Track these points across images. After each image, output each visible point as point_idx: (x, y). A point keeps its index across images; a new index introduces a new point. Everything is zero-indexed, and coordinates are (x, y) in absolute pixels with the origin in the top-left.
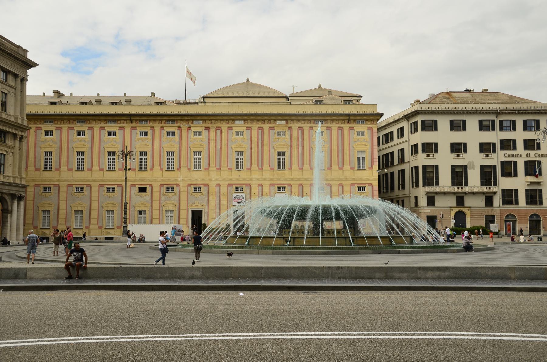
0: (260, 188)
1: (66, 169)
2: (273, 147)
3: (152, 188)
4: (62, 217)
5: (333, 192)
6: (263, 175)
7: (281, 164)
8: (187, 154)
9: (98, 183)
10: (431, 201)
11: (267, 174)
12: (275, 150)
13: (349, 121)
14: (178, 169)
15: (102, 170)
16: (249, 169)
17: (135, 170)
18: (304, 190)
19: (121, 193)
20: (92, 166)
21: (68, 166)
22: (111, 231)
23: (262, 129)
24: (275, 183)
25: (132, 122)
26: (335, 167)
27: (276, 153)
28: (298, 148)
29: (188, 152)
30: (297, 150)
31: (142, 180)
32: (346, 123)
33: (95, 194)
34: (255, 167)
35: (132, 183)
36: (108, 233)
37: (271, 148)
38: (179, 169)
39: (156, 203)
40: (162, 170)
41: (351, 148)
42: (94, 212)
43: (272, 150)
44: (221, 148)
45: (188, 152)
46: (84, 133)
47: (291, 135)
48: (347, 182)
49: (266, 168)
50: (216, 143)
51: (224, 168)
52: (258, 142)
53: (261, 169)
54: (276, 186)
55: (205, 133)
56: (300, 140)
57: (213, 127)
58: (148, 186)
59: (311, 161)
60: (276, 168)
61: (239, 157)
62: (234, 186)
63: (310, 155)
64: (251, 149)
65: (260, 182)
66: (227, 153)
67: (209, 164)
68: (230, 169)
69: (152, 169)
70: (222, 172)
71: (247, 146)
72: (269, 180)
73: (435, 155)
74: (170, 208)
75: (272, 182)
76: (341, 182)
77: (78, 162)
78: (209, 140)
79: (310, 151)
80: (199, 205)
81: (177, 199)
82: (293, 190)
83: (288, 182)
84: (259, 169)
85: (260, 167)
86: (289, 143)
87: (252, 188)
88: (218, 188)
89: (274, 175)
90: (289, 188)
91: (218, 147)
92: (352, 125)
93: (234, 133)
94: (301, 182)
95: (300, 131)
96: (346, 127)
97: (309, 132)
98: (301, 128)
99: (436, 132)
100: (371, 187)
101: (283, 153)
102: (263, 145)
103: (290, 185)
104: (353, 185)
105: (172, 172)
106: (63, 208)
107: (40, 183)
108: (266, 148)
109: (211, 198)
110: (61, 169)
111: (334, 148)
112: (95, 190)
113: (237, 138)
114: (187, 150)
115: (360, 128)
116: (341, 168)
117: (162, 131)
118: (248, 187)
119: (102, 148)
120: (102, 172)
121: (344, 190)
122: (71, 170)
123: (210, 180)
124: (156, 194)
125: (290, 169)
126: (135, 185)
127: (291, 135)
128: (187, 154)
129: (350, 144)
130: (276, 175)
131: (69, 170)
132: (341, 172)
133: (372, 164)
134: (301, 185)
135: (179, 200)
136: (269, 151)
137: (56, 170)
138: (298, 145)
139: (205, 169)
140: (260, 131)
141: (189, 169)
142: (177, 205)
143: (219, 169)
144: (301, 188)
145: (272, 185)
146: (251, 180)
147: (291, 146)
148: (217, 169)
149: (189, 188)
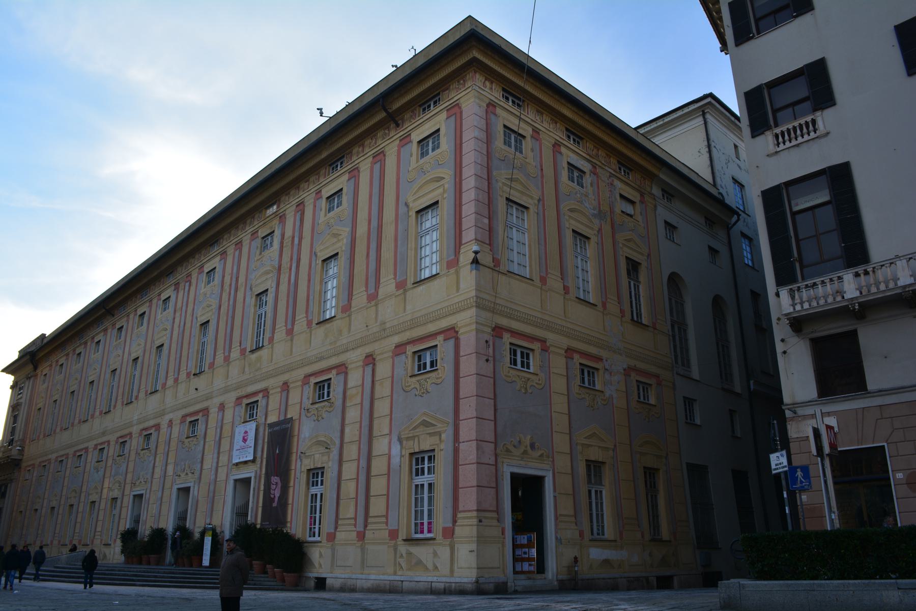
2: (251, 289)
5: (349, 393)
6: (227, 377)
10: (840, 370)
13: (394, 119)
25: (113, 316)
26: (360, 298)
28: (290, 269)
30: (287, 275)
41: (402, 209)
47: (283, 235)
52: (230, 285)
59: (311, 297)
63: (309, 281)
70: (179, 386)
73: (825, 119)
76: (368, 349)
78: (175, 311)
91: (182, 323)
99: (807, 19)
100: (451, 342)
104: (400, 349)
109: (157, 459)
111: (362, 230)
116: (373, 297)
123: (162, 414)
127: (283, 235)
133: (458, 244)
138: (291, 259)
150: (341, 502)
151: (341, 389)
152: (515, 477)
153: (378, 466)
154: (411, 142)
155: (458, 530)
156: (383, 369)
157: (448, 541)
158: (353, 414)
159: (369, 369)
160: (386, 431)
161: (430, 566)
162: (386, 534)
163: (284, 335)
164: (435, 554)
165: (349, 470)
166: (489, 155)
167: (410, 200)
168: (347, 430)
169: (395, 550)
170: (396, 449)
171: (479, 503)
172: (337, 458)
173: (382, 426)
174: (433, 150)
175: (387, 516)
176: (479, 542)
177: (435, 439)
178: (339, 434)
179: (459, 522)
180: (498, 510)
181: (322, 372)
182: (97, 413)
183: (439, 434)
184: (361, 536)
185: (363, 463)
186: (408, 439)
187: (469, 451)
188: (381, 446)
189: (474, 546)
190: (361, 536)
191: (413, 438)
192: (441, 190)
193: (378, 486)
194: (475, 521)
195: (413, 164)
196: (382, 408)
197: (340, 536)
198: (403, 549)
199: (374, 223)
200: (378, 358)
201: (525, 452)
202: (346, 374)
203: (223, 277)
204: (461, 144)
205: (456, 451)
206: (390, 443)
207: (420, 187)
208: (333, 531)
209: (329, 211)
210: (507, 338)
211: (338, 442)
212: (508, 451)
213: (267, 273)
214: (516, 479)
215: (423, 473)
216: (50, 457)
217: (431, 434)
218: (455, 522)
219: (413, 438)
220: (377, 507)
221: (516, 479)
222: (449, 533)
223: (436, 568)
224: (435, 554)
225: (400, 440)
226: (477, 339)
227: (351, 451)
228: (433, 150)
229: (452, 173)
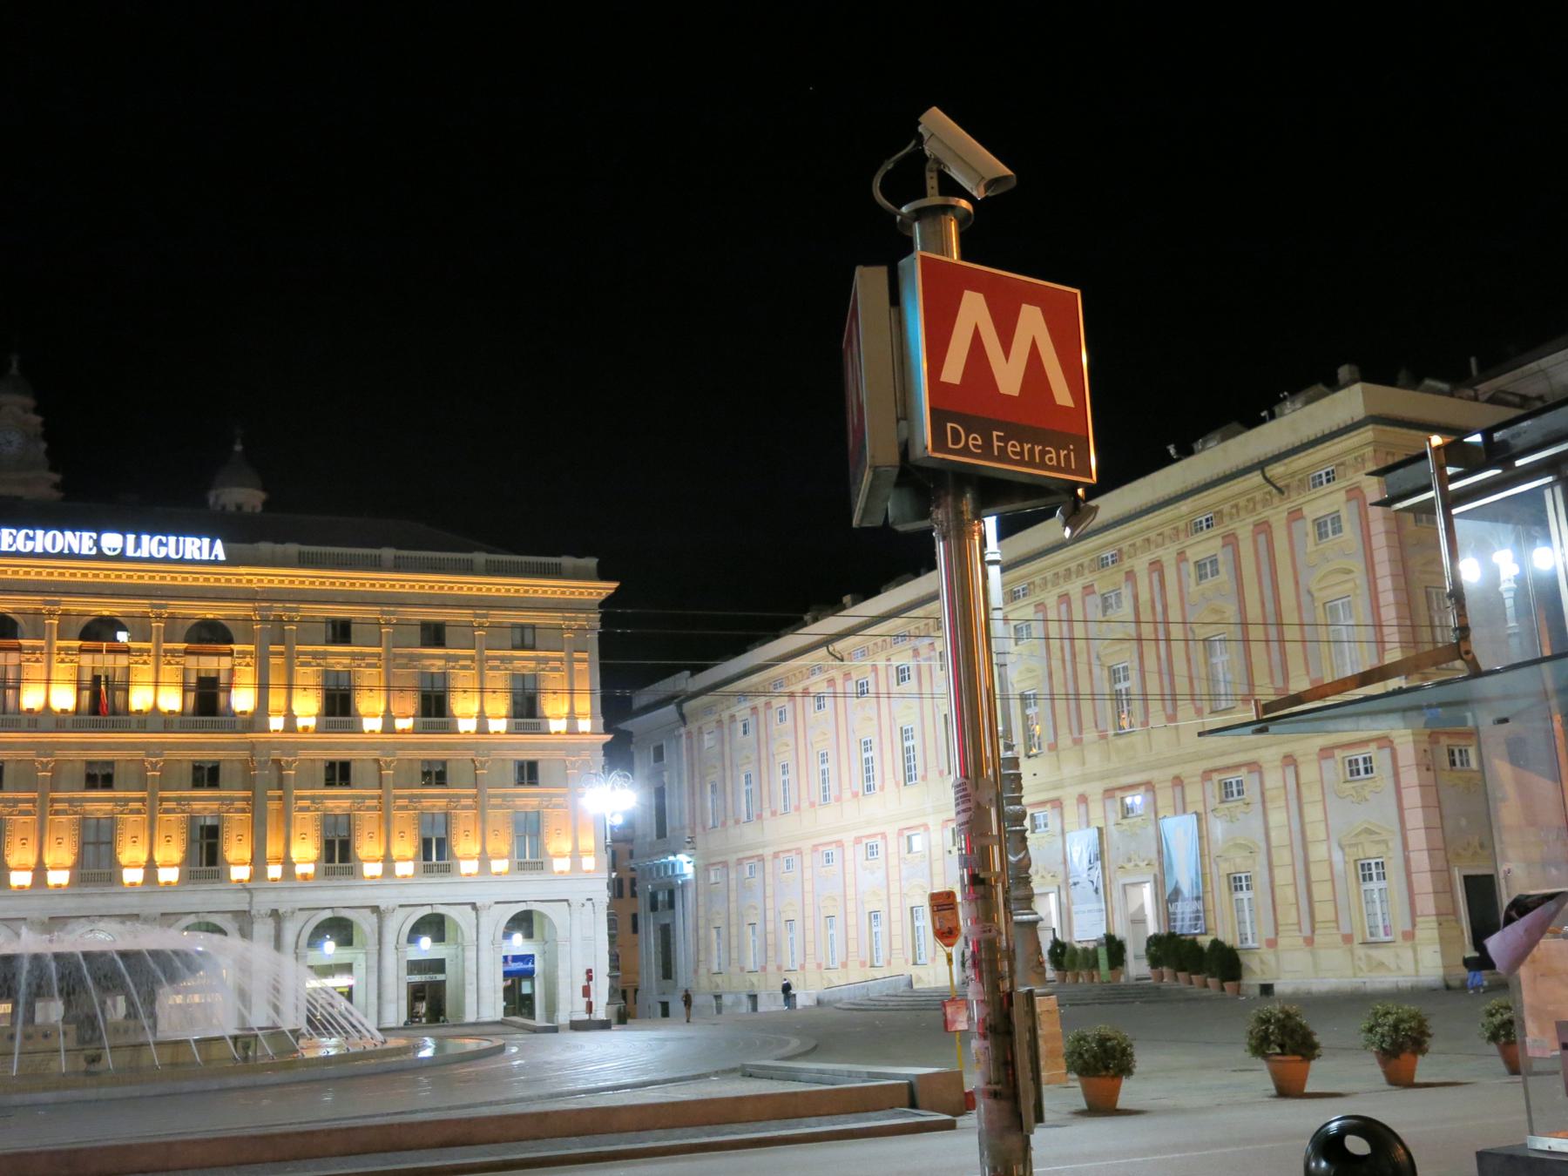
2: (1098, 658)
4: (770, 938)
5: (1268, 794)
18: (1188, 799)
27: (1106, 672)
32: (1276, 500)
34: (1065, 740)
35: (855, 834)
37: (1093, 656)
39: (894, 888)
40: (897, 784)
41: (1305, 599)
42: (809, 924)
43: (1096, 670)
47: (1136, 598)
49: (1090, 735)
58: (879, 841)
60: (1111, 732)
63: (1189, 660)
69: (882, 788)
72: (1102, 778)
82: (1159, 804)
85: (1076, 735)
94: (1175, 771)
96: (1277, 514)
97: (1179, 570)
98: (1157, 566)
100: (1387, 752)
106: (770, 915)
107: (741, 855)
115: (1322, 502)
118: (1057, 811)
121: (1303, 780)
124: (893, 861)
127: (1136, 598)
129: (1297, 583)
136: (1090, 672)
144: (1178, 789)
146: (1057, 786)
150: (1279, 909)
152: (1467, 879)
153: (1319, 872)
154: (1302, 517)
155: (1418, 933)
156: (1309, 772)
157: (1409, 944)
158: (1277, 817)
160: (1323, 836)
161: (1393, 966)
162: (1339, 938)
163: (1162, 721)
164: (1397, 956)
165: (1283, 876)
166: (1401, 544)
167: (1313, 589)
168: (1273, 834)
169: (1352, 952)
170: (1337, 856)
171: (1437, 907)
172: (1265, 862)
173: (1316, 831)
174: (1334, 533)
175: (1336, 921)
176: (1441, 943)
177: (1382, 848)
178: (1263, 837)
179: (1419, 926)
180: (1455, 912)
181: (1227, 769)
182: (847, 795)
183: (1385, 842)
184: (1310, 941)
185: (1300, 867)
186: (1351, 845)
187: (1421, 860)
188: (1318, 852)
189: (1437, 948)
190: (1310, 941)
191: (1356, 845)
192: (1350, 585)
193: (1321, 892)
194: (1435, 925)
195: (1311, 547)
196: (1313, 813)
197: (1283, 942)
198: (1361, 951)
200: (1300, 759)
201: (1475, 853)
202: (1261, 774)
204: (1369, 536)
205: (1407, 860)
206: (1329, 849)
207: (1325, 576)
208: (1272, 936)
209: (1201, 577)
210: (1445, 741)
211: (1263, 845)
212: (1458, 855)
214: (1469, 881)
215: (1371, 879)
216: (760, 852)
217: (1378, 842)
218: (1414, 925)
219: (1356, 845)
220: (1324, 912)
221: (1469, 881)
222: (1409, 936)
223: (1399, 968)
224: (1397, 956)
225: (1342, 848)
226: (1416, 750)
227: (1282, 857)
228: (1334, 533)
229: (1362, 567)
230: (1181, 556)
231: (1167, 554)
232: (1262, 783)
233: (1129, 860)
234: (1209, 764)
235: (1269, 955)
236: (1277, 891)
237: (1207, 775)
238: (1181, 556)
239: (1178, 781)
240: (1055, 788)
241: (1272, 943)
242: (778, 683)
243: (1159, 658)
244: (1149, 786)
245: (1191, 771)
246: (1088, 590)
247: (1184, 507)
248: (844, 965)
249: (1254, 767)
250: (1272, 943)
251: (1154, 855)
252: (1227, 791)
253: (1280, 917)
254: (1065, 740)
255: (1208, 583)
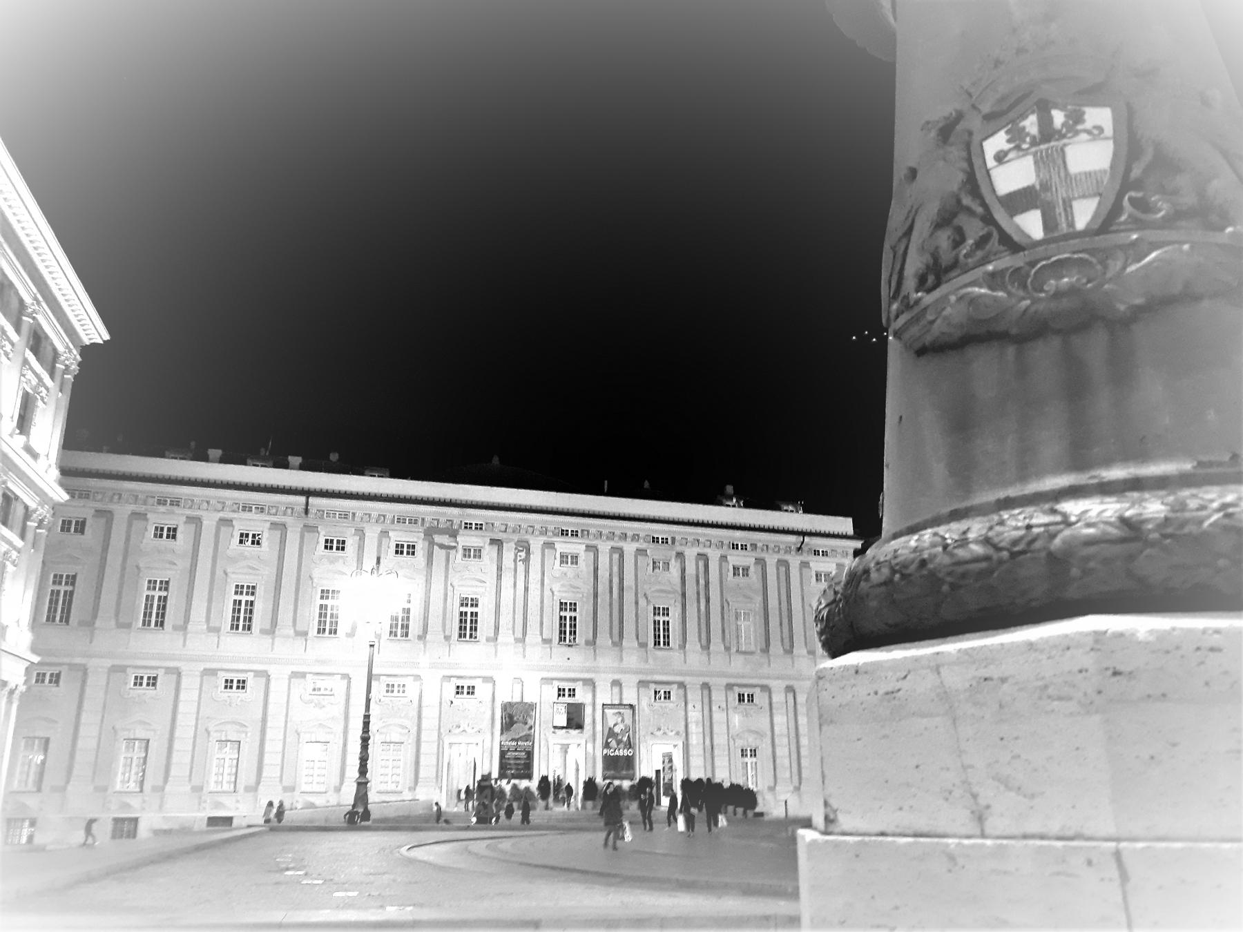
0: (616, 690)
1: (113, 623)
3: (349, 682)
6: (621, 659)
7: (661, 638)
8: (446, 599)
9: (202, 667)
11: (632, 659)
12: (648, 602)
14: (420, 638)
15: (217, 630)
16: (592, 643)
17: (305, 634)
19: (262, 694)
20: (187, 619)
21: (117, 615)
22: (228, 801)
23: (621, 552)
24: (649, 678)
26: (776, 647)
28: (698, 602)
29: (446, 595)
30: (695, 605)
31: (323, 662)
33: (189, 696)
34: (604, 639)
35: (295, 669)
36: (218, 805)
38: (422, 637)
43: (642, 602)
44: (526, 589)
45: (446, 595)
46: (172, 534)
47: (683, 570)
48: (802, 683)
49: (629, 642)
50: (515, 577)
51: (533, 636)
52: (611, 581)
53: (618, 644)
54: (653, 687)
55: (489, 553)
56: (702, 582)
57: (509, 541)
61: (568, 614)
62: (556, 684)
63: (723, 618)
64: (596, 595)
65: (616, 677)
66: (542, 602)
67: (497, 628)
68: (547, 641)
71: (588, 588)
74: (395, 737)
75: (644, 678)
77: (149, 606)
78: (500, 569)
79: (723, 608)
80: (469, 730)
81: (415, 714)
82: (689, 697)
83: (679, 679)
84: (614, 644)
85: (616, 638)
86: (678, 588)
87: (598, 690)
88: (518, 687)
89: (647, 661)
90: (681, 692)
92: (805, 557)
93: (558, 556)
94: (707, 680)
95: (701, 564)
96: (795, 561)
101: (666, 612)
102: (621, 589)
103: (682, 685)
105: (404, 644)
108: (629, 597)
110: (98, 623)
112: (190, 684)
113: (565, 568)
114: (446, 589)
116: (789, 651)
117: (385, 541)
119: (219, 573)
120: (213, 638)
122: (128, 626)
125: (683, 646)
126: (303, 675)
127: (683, 570)
128: (446, 599)
130: (651, 661)
131: (120, 626)
132: (789, 661)
134: (706, 687)
135: (420, 717)
136: (637, 603)
137: (81, 623)
138: (698, 594)
139: (488, 640)
140: (616, 556)
141: (447, 638)
142: (414, 730)
143: (523, 640)
144: (706, 692)
145: (643, 684)
146: (595, 670)
147: (684, 595)
148: (517, 640)
149: (445, 684)
151: (767, 702)
158: (780, 720)
159: (790, 696)
165: (782, 752)
168: (776, 728)
172: (769, 742)
184: (798, 789)
199: (784, 604)
203: (596, 570)
211: (769, 733)
213: (669, 592)
230: (724, 558)
231: (714, 555)
232: (770, 698)
233: (659, 729)
234: (732, 681)
235: (769, 796)
236: (778, 761)
237: (729, 687)
238: (724, 558)
239: (706, 687)
240: (588, 671)
241: (772, 789)
242: (191, 503)
243: (699, 610)
244: (682, 685)
245: (718, 683)
246: (641, 552)
247: (738, 534)
248: (253, 789)
249: (765, 688)
250: (772, 789)
251: (682, 728)
252: (741, 698)
253: (778, 775)
254: (604, 639)
255: (741, 580)
